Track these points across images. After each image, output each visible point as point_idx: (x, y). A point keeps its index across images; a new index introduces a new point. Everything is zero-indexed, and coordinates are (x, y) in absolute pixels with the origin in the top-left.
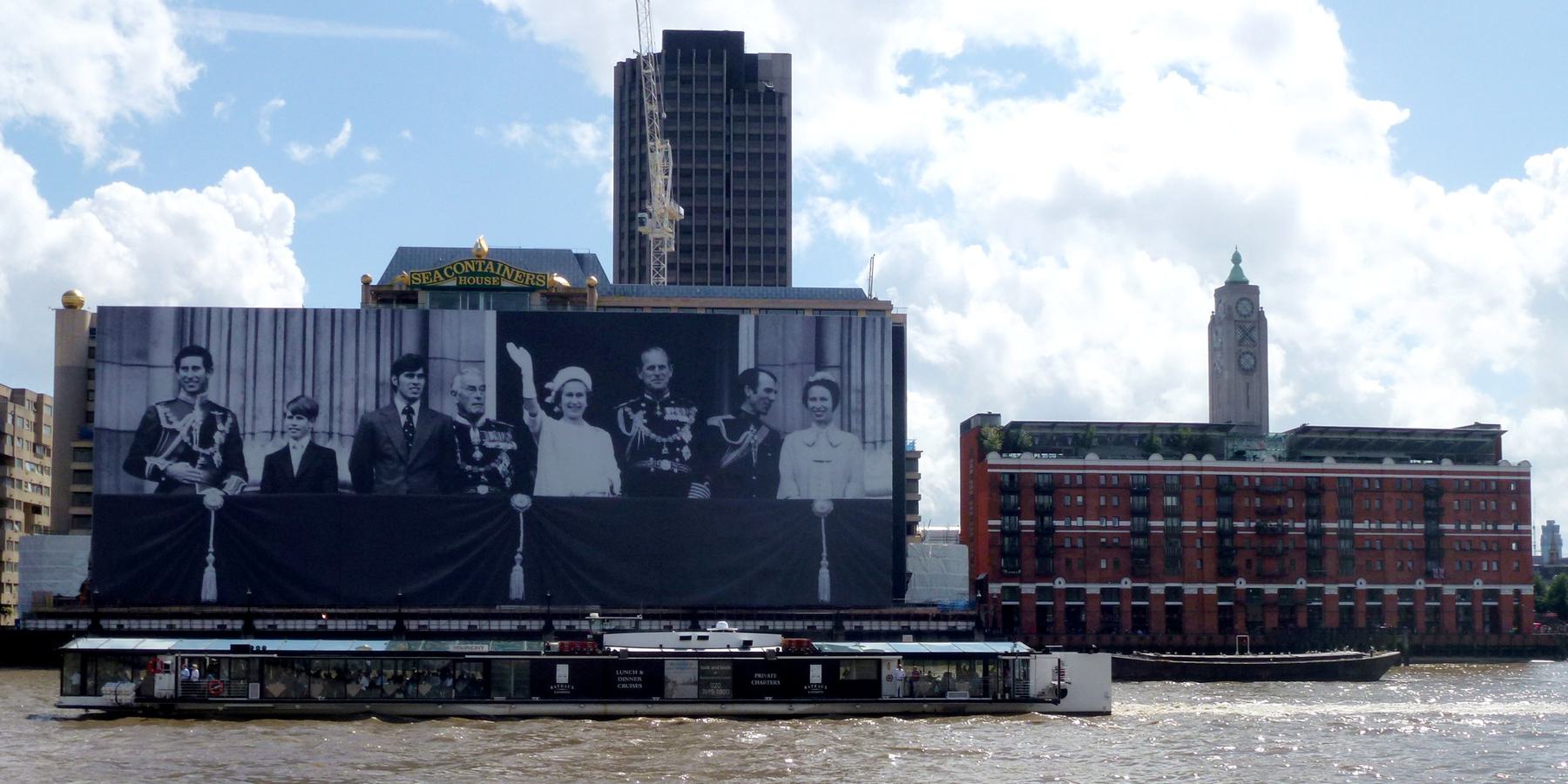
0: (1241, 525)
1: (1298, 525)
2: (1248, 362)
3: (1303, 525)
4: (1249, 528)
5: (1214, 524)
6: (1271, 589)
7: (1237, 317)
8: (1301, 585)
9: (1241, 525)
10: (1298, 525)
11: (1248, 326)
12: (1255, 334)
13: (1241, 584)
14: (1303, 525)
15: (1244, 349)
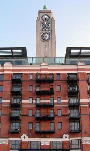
0: (27, 101)
1: (63, 101)
2: (46, 36)
3: (67, 101)
4: (32, 104)
5: (8, 101)
6: (46, 141)
7: (41, 20)
8: (66, 138)
9: (27, 101)
10: (63, 101)
11: (46, 23)
12: (49, 26)
13: (25, 138)
14: (67, 101)
15: (44, 32)
